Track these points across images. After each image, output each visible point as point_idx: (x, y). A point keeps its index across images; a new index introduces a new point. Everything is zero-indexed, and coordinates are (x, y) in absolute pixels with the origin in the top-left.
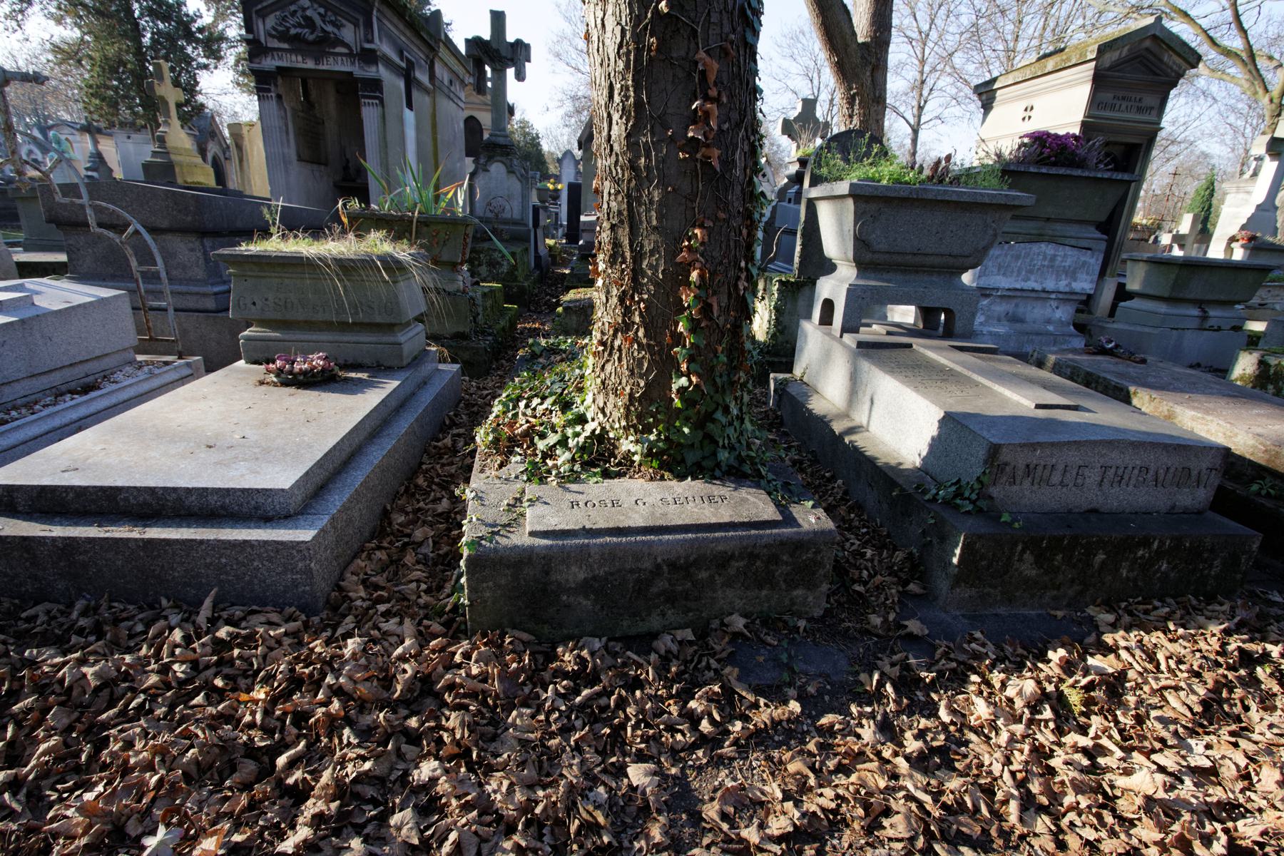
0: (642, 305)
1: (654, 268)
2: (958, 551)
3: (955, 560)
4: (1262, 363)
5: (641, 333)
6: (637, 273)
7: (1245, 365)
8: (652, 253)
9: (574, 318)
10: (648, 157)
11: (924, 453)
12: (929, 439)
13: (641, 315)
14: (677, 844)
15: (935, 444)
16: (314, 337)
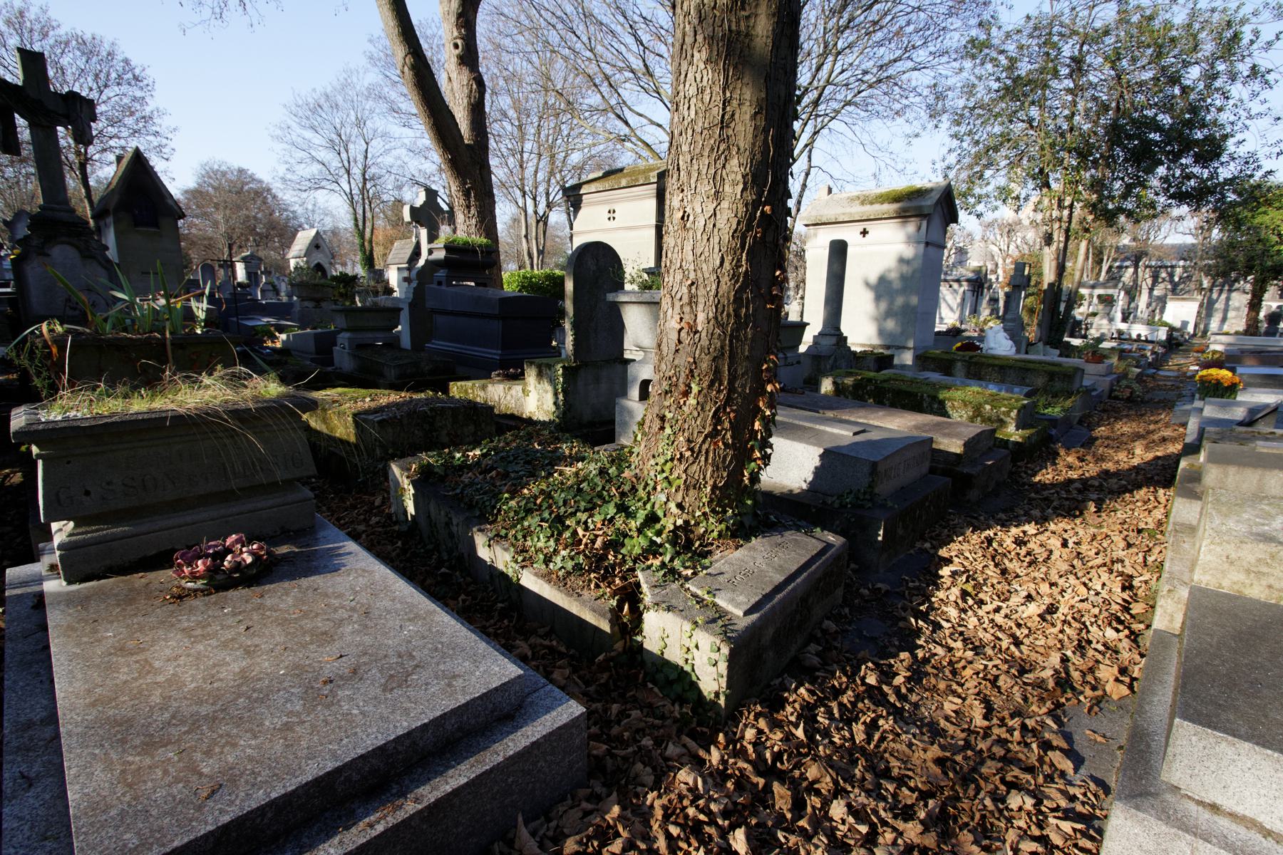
0: (732, 415)
1: (744, 386)
2: (881, 532)
3: (880, 538)
4: (834, 383)
5: (728, 436)
6: (731, 389)
7: (827, 386)
8: (743, 375)
9: (390, 430)
10: (748, 309)
11: (810, 478)
12: (812, 469)
13: (730, 422)
14: (761, 842)
15: (817, 472)
16: (189, 519)
